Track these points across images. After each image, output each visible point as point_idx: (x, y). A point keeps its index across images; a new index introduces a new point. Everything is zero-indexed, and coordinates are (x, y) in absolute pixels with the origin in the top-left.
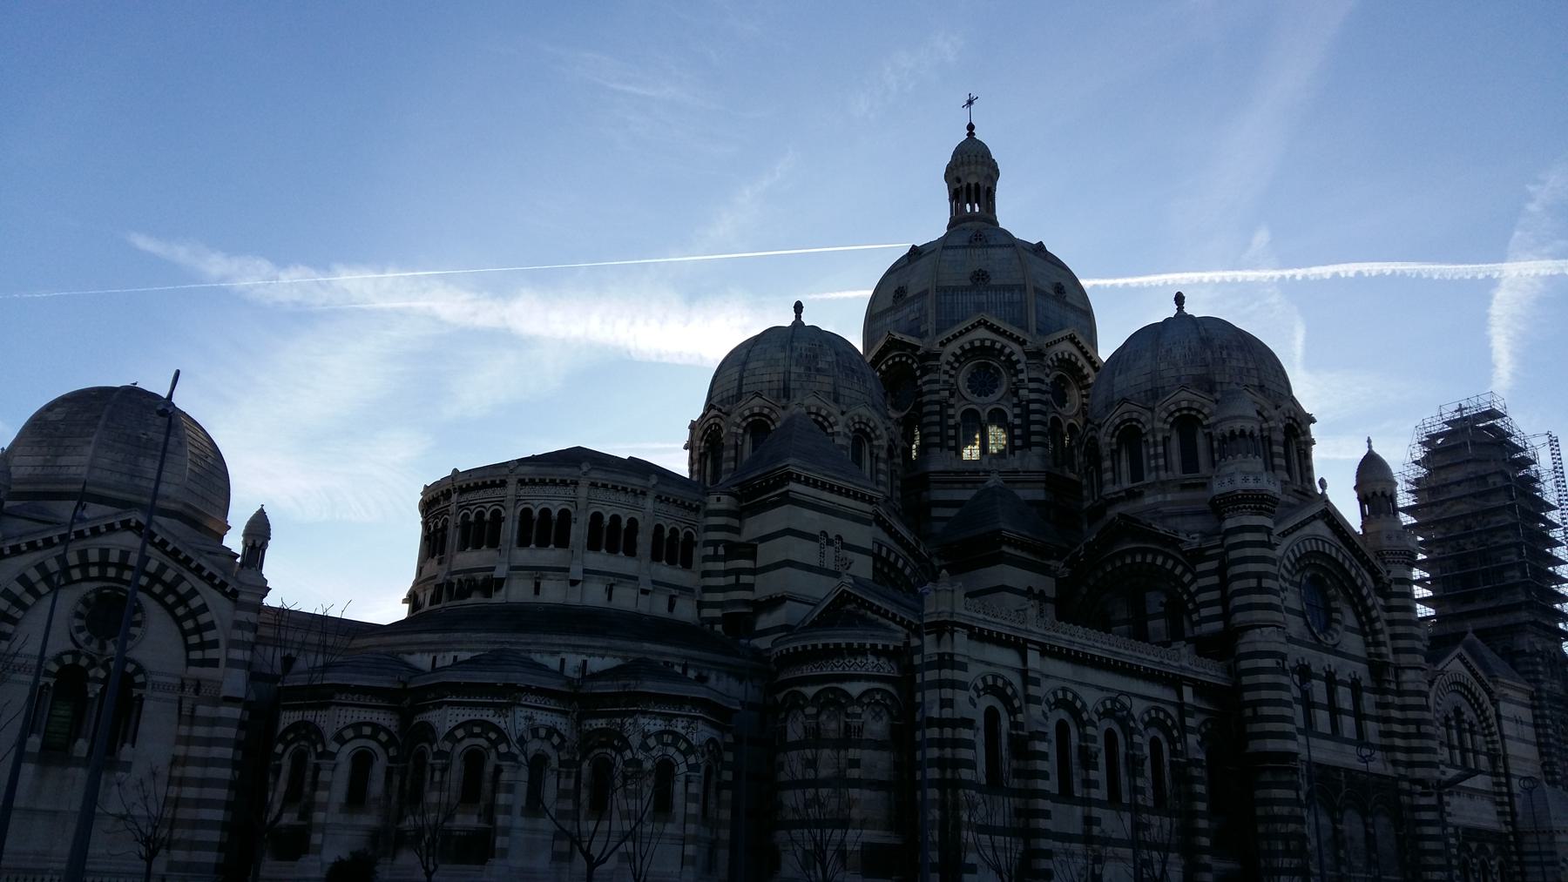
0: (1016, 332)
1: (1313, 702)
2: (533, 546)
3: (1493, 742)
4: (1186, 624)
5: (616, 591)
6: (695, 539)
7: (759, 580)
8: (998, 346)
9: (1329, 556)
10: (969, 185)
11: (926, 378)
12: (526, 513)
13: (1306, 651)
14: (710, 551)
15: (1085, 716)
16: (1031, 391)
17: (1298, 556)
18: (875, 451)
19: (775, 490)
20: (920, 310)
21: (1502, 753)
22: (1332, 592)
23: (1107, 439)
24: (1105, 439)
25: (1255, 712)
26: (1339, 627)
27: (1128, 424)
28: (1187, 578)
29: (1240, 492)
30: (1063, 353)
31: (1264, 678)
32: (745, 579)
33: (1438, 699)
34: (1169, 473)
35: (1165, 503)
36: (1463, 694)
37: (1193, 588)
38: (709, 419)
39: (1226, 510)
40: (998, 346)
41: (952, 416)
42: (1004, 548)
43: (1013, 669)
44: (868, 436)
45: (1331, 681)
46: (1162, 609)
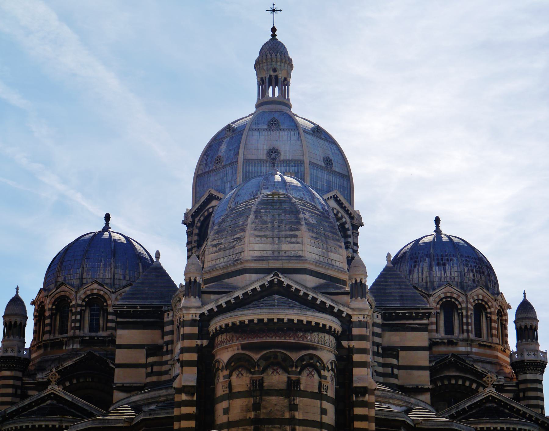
7: (400, 373)
27: (449, 299)
29: (540, 362)
35: (471, 352)
39: (529, 368)
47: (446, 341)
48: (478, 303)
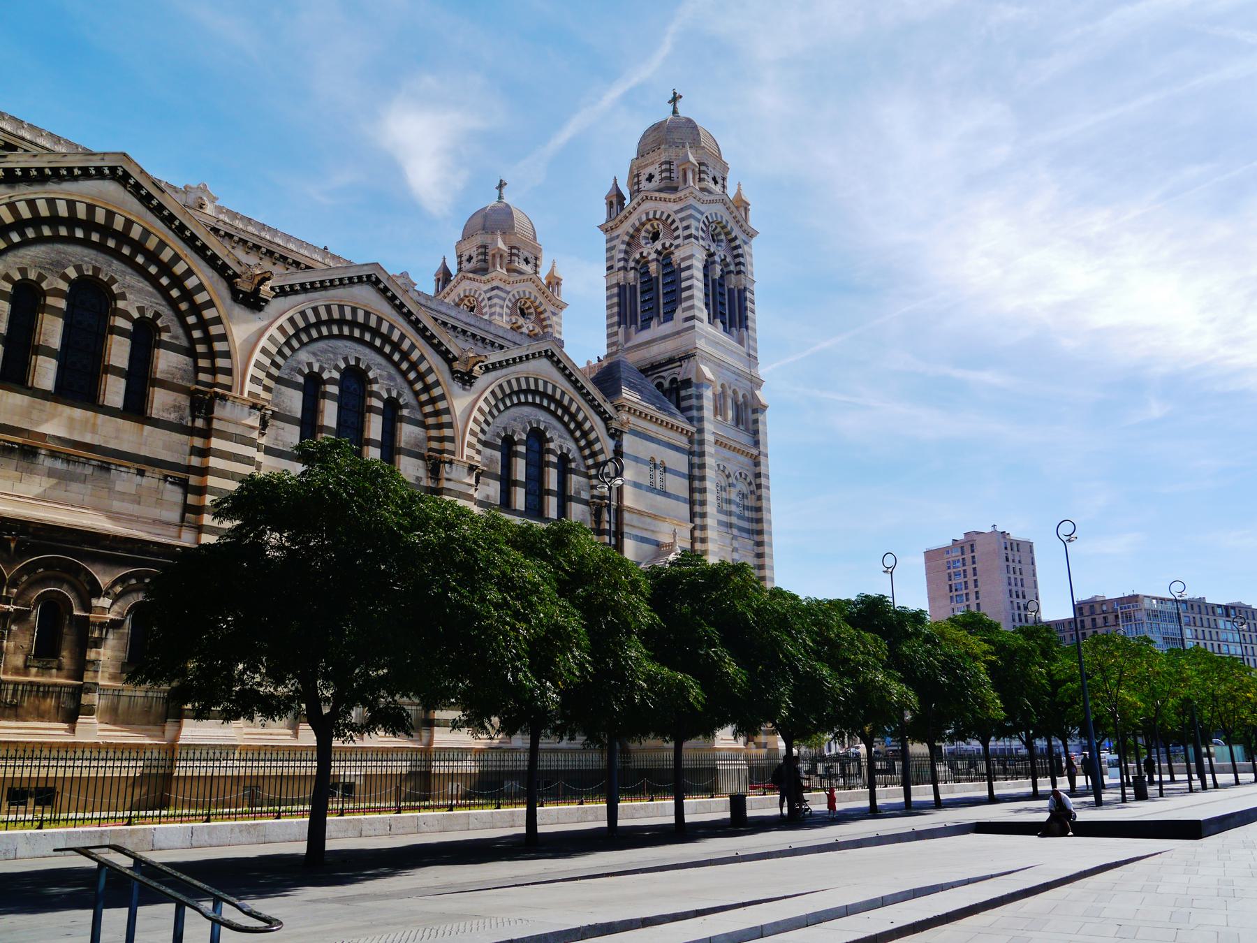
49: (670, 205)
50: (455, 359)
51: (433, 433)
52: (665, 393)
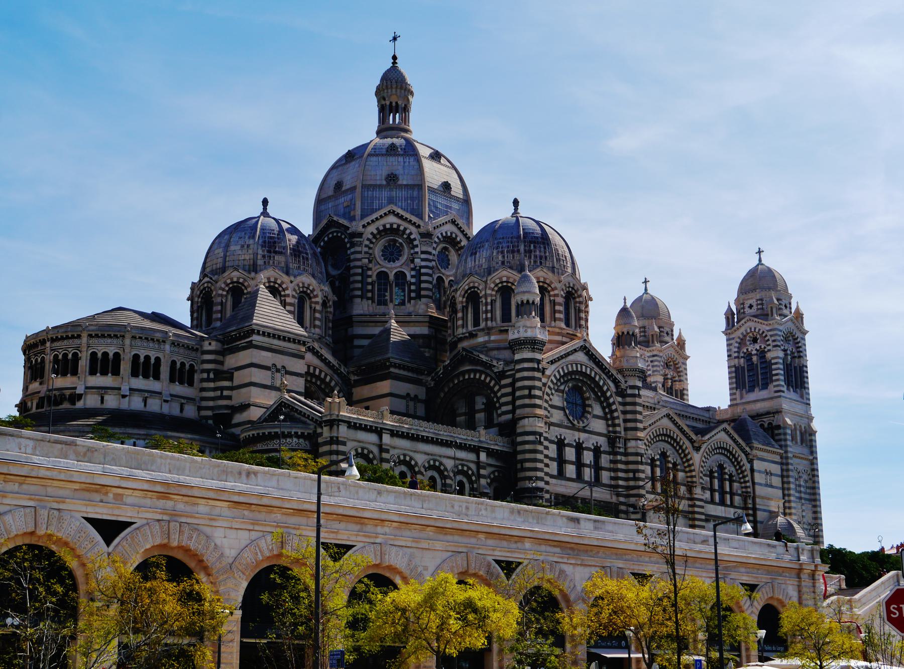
0: (414, 219)
1: (565, 460)
2: (98, 374)
3: (746, 487)
4: (495, 415)
5: (149, 401)
6: (196, 368)
7: (234, 393)
8: (402, 228)
9: (585, 373)
10: (391, 103)
11: (352, 250)
12: (94, 355)
13: (563, 430)
14: (205, 375)
15: (417, 469)
16: (423, 260)
17: (562, 374)
18: (313, 305)
19: (244, 339)
20: (351, 200)
21: (752, 495)
22: (587, 395)
23: (461, 299)
24: (460, 299)
25: (522, 466)
26: (589, 416)
28: (497, 388)
30: (446, 233)
31: (527, 447)
32: (225, 393)
33: (703, 459)
34: (494, 323)
35: (489, 341)
36: (726, 456)
37: (499, 394)
38: (204, 284)
40: (402, 228)
41: (370, 276)
42: (392, 370)
43: (374, 444)
44: (308, 295)
45: (579, 448)
46: (483, 407)
47: (467, 335)
48: (503, 286)
49: (764, 326)
50: (695, 441)
51: (689, 474)
52: (765, 430)
